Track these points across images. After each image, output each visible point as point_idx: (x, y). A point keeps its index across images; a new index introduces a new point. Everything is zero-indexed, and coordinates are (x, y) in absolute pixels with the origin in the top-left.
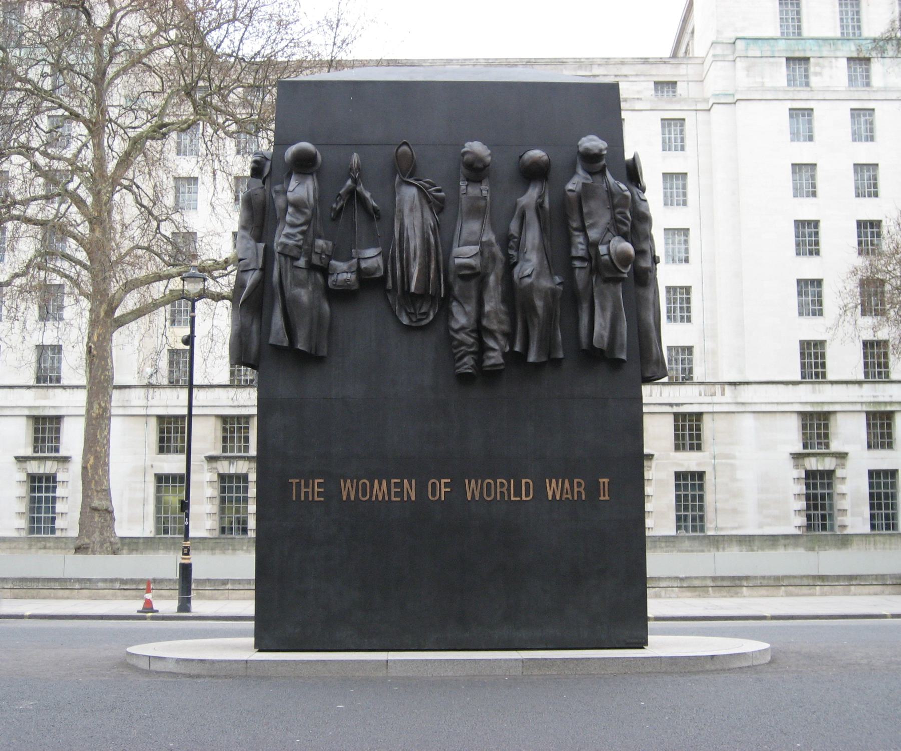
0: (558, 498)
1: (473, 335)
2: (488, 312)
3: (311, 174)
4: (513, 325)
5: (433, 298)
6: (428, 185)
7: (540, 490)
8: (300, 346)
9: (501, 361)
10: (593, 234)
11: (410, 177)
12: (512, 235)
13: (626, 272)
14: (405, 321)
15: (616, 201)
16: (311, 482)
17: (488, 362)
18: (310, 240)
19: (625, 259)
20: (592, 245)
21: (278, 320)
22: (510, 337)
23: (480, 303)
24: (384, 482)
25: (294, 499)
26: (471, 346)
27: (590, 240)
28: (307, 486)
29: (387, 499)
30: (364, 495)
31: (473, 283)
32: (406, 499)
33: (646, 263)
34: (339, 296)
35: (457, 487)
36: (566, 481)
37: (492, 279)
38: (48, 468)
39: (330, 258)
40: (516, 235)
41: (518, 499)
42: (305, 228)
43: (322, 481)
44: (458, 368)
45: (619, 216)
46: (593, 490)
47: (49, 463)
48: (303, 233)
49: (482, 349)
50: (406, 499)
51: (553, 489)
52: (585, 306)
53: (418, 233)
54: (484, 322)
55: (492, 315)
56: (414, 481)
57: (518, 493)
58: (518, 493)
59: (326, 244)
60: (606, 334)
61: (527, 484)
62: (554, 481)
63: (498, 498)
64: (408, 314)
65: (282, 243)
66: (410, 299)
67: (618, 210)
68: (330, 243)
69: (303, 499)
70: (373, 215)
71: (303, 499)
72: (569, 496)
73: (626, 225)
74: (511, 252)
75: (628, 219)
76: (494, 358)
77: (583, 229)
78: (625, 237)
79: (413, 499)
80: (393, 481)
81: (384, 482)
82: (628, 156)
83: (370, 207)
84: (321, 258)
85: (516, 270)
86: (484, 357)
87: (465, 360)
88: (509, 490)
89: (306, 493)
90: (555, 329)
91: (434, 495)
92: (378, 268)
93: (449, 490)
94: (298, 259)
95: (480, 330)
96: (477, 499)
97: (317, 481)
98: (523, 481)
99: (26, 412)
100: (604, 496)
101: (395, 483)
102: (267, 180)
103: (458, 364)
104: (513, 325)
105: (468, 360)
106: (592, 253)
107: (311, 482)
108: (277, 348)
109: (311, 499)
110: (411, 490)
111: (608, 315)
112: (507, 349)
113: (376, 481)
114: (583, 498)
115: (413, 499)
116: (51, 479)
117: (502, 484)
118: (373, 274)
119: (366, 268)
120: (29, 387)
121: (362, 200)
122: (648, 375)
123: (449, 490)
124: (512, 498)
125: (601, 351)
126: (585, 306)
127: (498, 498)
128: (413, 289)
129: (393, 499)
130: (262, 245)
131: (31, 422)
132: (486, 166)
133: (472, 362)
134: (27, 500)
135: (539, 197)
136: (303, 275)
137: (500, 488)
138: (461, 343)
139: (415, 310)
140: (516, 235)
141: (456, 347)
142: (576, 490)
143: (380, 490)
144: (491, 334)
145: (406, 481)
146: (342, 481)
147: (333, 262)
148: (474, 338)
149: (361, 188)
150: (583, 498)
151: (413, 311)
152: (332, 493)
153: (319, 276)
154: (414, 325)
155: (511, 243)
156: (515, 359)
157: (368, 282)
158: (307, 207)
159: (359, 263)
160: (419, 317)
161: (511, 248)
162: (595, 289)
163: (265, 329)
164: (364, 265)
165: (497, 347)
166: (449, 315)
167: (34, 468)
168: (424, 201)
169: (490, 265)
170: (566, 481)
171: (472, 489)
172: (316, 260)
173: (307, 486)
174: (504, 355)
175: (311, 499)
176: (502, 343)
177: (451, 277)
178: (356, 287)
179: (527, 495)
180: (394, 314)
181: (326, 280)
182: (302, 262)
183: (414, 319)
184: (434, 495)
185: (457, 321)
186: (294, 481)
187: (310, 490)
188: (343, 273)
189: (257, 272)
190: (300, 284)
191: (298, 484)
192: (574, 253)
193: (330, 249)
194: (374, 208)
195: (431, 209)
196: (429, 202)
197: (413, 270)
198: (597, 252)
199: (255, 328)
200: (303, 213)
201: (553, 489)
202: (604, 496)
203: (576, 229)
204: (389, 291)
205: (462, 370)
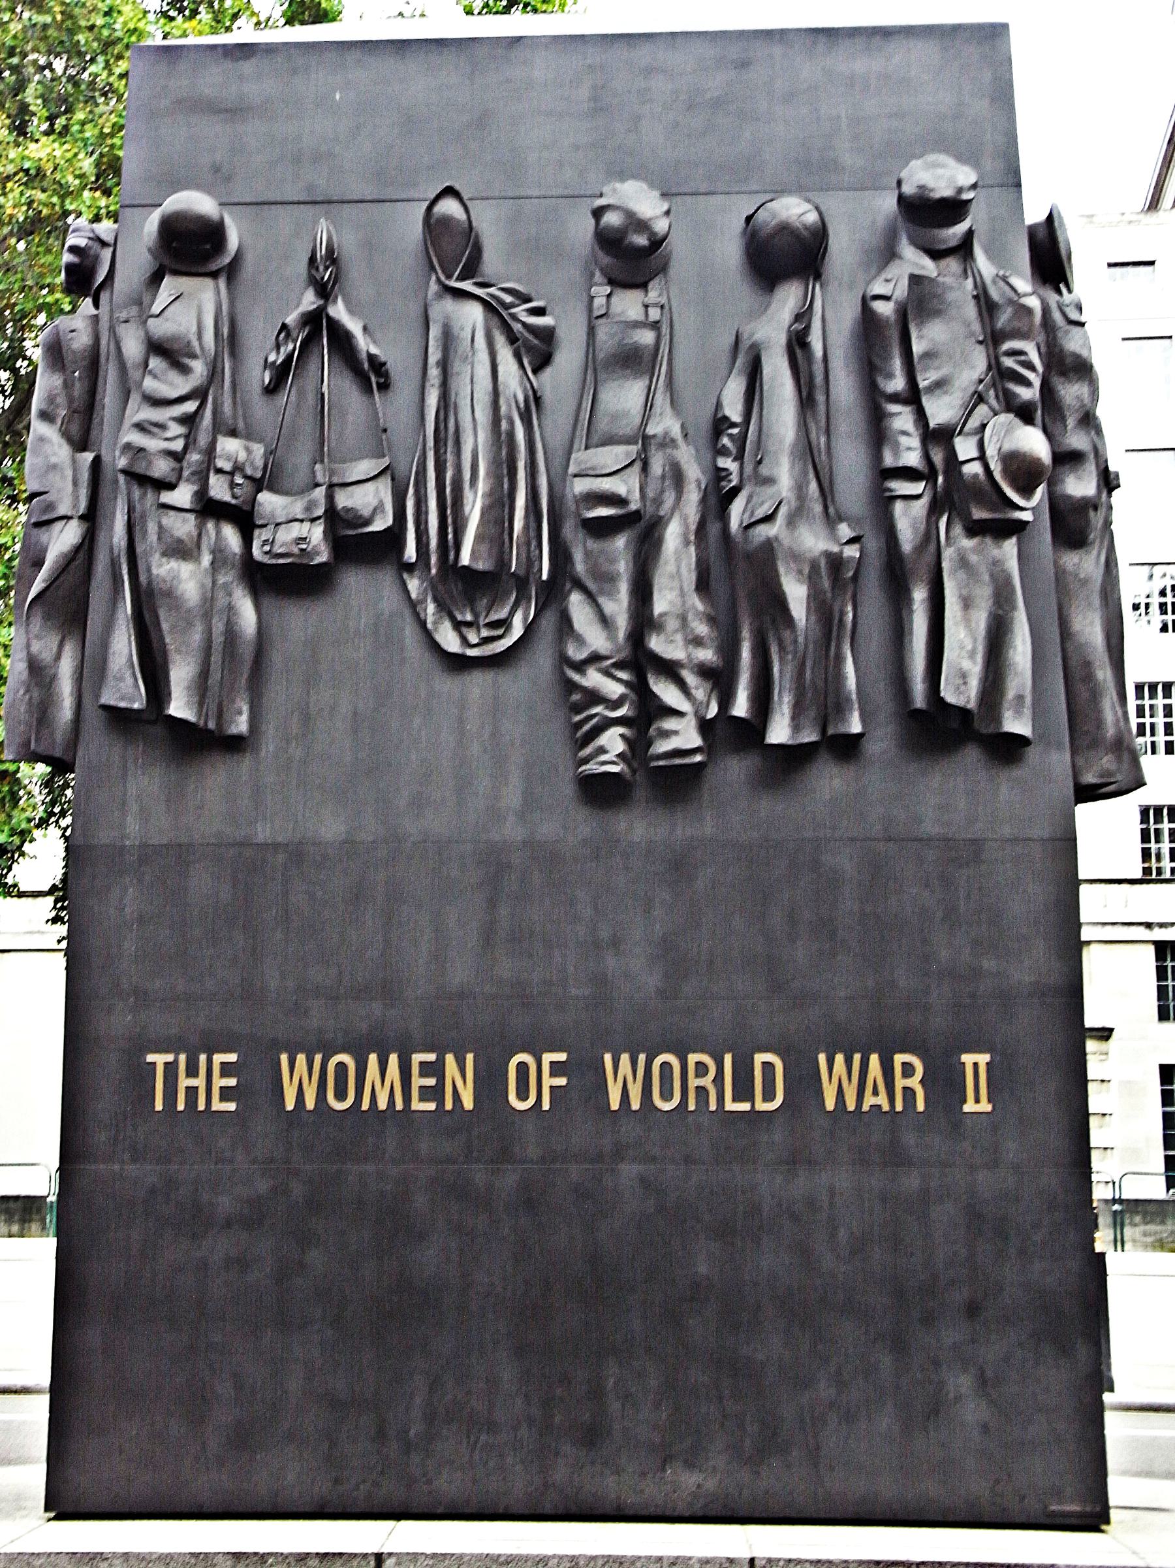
0: (851, 1106)
1: (624, 675)
2: (661, 615)
3: (214, 275)
4: (729, 650)
5: (521, 583)
6: (508, 299)
7: (804, 1083)
8: (179, 707)
9: (696, 741)
10: (940, 411)
11: (461, 278)
12: (726, 418)
13: (1031, 507)
14: (450, 641)
15: (1003, 319)
16: (203, 1058)
17: (663, 746)
18: (203, 439)
19: (1025, 473)
20: (938, 437)
21: (123, 646)
22: (720, 679)
23: (642, 592)
24: (393, 1059)
25: (159, 1106)
26: (616, 704)
27: (932, 424)
28: (192, 1072)
29: (399, 1106)
30: (341, 1095)
31: (620, 542)
32: (449, 1106)
33: (1080, 485)
34: (282, 580)
36: (874, 1059)
37: (672, 535)
39: (259, 485)
40: (736, 418)
41: (745, 1106)
42: (190, 406)
43: (232, 1057)
44: (586, 761)
45: (1009, 362)
46: (945, 1083)
48: (189, 421)
49: (647, 714)
50: (449, 1106)
52: (919, 595)
53: (483, 415)
54: (656, 643)
55: (672, 624)
56: (470, 1057)
57: (743, 1091)
58: (743, 1091)
59: (248, 450)
60: (975, 669)
62: (839, 1058)
64: (458, 626)
65: (128, 446)
66: (464, 588)
67: (1007, 345)
68: (259, 450)
69: (181, 1107)
70: (372, 376)
71: (181, 1107)
72: (882, 1100)
73: (1027, 383)
74: (726, 463)
75: (1030, 366)
76: (684, 735)
77: (913, 397)
78: (1025, 414)
79: (468, 1103)
80: (417, 1058)
81: (393, 1059)
82: (1034, 214)
83: (364, 356)
84: (232, 485)
85: (737, 512)
86: (652, 731)
87: (604, 739)
88: (719, 1079)
89: (192, 1092)
90: (839, 660)
91: (522, 1095)
92: (378, 509)
93: (562, 1081)
94: (171, 487)
95: (640, 662)
96: (635, 1105)
97: (218, 1058)
98: (760, 1058)
100: (977, 1101)
101: (422, 1064)
102: (104, 297)
103: (588, 750)
104: (729, 650)
105: (613, 741)
106: (938, 457)
107: (203, 1058)
108: (118, 717)
109: (201, 1107)
111: (981, 618)
112: (713, 711)
113: (373, 1058)
114: (921, 1107)
115: (468, 1103)
117: (701, 1069)
118: (368, 522)
119: (347, 510)
121: (342, 341)
122: (1090, 778)
123: (562, 1081)
124: (730, 1106)
125: (963, 713)
126: (919, 595)
128: (465, 559)
129: (417, 1105)
130: (89, 456)
132: (657, 243)
133: (620, 747)
135: (798, 317)
136: (183, 527)
137: (700, 1079)
138: (594, 697)
139: (476, 615)
140: (736, 418)
141: (577, 708)
142: (900, 1083)
143: (382, 1084)
144: (670, 670)
145: (450, 1058)
146: (284, 1058)
147: (265, 497)
148: (627, 684)
149: (338, 310)
150: (921, 1107)
151: (469, 617)
152: (257, 1086)
153: (231, 536)
154: (471, 652)
155: (725, 441)
156: (732, 735)
157: (356, 544)
158: (193, 356)
159: (330, 498)
160: (485, 633)
161: (724, 452)
162: (948, 555)
163: (92, 671)
164: (343, 500)
165: (684, 705)
166: (565, 624)
168: (500, 340)
169: (669, 499)
170: (874, 1059)
172: (219, 489)
174: (705, 727)
175: (201, 1107)
176: (700, 694)
177: (569, 530)
178: (323, 557)
180: (423, 624)
181: (247, 540)
182: (182, 496)
183: (473, 638)
185: (580, 640)
186: (159, 1059)
187: (200, 1082)
188: (292, 527)
189: (74, 523)
190: (182, 551)
191: (171, 1068)
192: (889, 461)
193: (260, 463)
194: (371, 358)
195: (518, 356)
196: (512, 339)
197: (467, 509)
198: (951, 454)
199: (66, 668)
200: (185, 370)
201: (835, 1079)
203: (895, 398)
204: (410, 568)
205: (592, 767)
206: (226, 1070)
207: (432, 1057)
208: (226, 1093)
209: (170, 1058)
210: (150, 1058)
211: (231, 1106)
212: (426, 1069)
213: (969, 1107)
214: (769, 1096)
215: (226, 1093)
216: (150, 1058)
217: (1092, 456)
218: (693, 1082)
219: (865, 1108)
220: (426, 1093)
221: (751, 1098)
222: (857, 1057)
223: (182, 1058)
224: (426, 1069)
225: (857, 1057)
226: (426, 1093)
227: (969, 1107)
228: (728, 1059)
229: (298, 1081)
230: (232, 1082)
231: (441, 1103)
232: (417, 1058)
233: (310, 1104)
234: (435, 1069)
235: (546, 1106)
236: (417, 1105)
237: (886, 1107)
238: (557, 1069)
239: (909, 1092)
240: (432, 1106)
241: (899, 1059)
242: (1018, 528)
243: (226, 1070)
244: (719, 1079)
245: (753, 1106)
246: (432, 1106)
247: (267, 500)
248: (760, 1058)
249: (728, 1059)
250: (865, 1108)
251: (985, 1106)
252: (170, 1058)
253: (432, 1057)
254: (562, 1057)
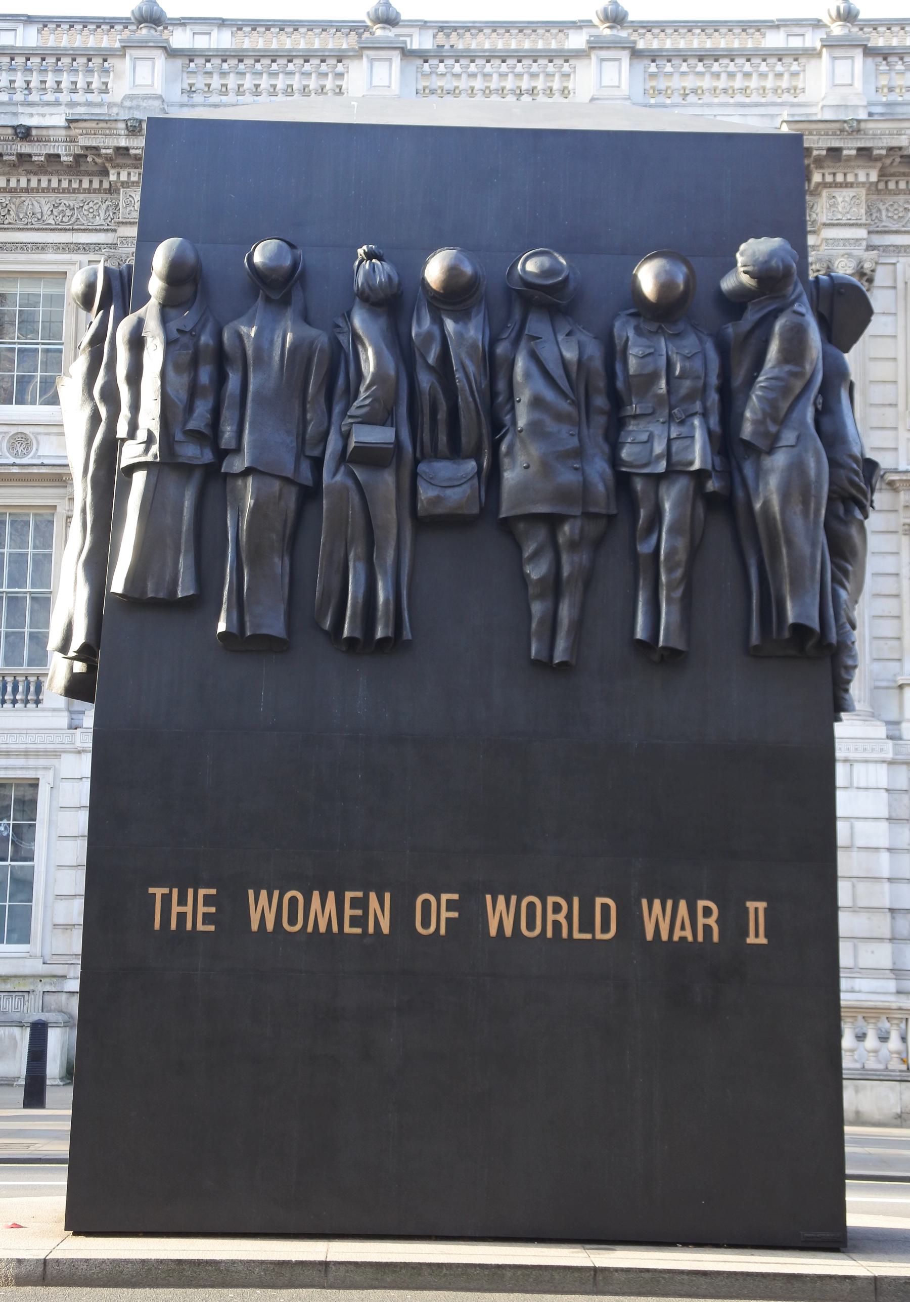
0: (665, 937)
7: (630, 921)
16: (191, 892)
24: (331, 895)
25: (157, 925)
28: (182, 901)
29: (335, 929)
32: (371, 930)
36: (683, 905)
41: (588, 936)
46: (733, 922)
50: (371, 930)
51: (658, 919)
56: (387, 896)
57: (587, 925)
58: (587, 925)
61: (605, 907)
63: (549, 934)
79: (386, 929)
80: (349, 895)
81: (331, 895)
88: (569, 917)
89: (182, 917)
91: (426, 924)
93: (455, 915)
97: (202, 892)
98: (599, 901)
107: (191, 892)
110: (381, 915)
113: (316, 895)
114: (716, 938)
115: (386, 929)
117: (557, 908)
123: (455, 915)
124: (577, 935)
127: (549, 934)
129: (347, 929)
137: (556, 914)
142: (701, 921)
143: (322, 912)
145: (373, 896)
150: (716, 938)
170: (683, 905)
171: (499, 914)
173: (182, 901)
175: (189, 926)
179: (605, 928)
184: (426, 924)
186: (158, 892)
187: (188, 909)
191: (167, 899)
202: (757, 935)
206: (208, 901)
207: (360, 894)
208: (207, 918)
209: (166, 891)
210: (151, 890)
211: (212, 928)
212: (355, 903)
213: (751, 940)
214: (605, 928)
215: (207, 918)
216: (151, 890)
218: (551, 917)
219: (676, 938)
220: (354, 921)
221: (592, 930)
222: (669, 903)
223: (175, 891)
224: (355, 903)
225: (669, 903)
226: (354, 921)
227: (751, 940)
228: (576, 901)
229: (262, 909)
230: (213, 910)
231: (365, 926)
232: (349, 895)
233: (270, 927)
234: (361, 903)
235: (443, 931)
236: (347, 929)
237: (690, 939)
238: (451, 905)
239: (707, 929)
240: (358, 931)
241: (701, 904)
243: (208, 901)
244: (569, 917)
245: (594, 936)
246: (358, 931)
248: (599, 901)
249: (576, 901)
250: (676, 938)
251: (762, 940)
252: (166, 891)
253: (360, 894)
254: (455, 896)
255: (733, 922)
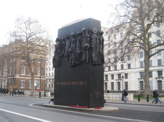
7: (79, 83)
19: (87, 47)
22: (75, 60)
35: (71, 83)
38: (160, 79)
46: (84, 83)
47: (160, 79)
51: (81, 83)
78: (88, 42)
99: (139, 72)
116: (161, 81)
120: (157, 66)
131: (157, 72)
134: (157, 85)
167: (158, 79)
217: (94, 44)
229: (61, 83)
234: (66, 83)
242: (87, 50)
247: (60, 53)
255: (84, 83)
